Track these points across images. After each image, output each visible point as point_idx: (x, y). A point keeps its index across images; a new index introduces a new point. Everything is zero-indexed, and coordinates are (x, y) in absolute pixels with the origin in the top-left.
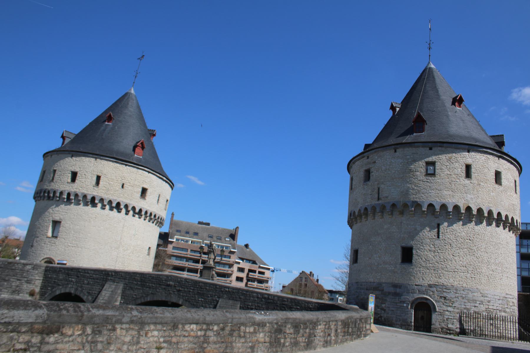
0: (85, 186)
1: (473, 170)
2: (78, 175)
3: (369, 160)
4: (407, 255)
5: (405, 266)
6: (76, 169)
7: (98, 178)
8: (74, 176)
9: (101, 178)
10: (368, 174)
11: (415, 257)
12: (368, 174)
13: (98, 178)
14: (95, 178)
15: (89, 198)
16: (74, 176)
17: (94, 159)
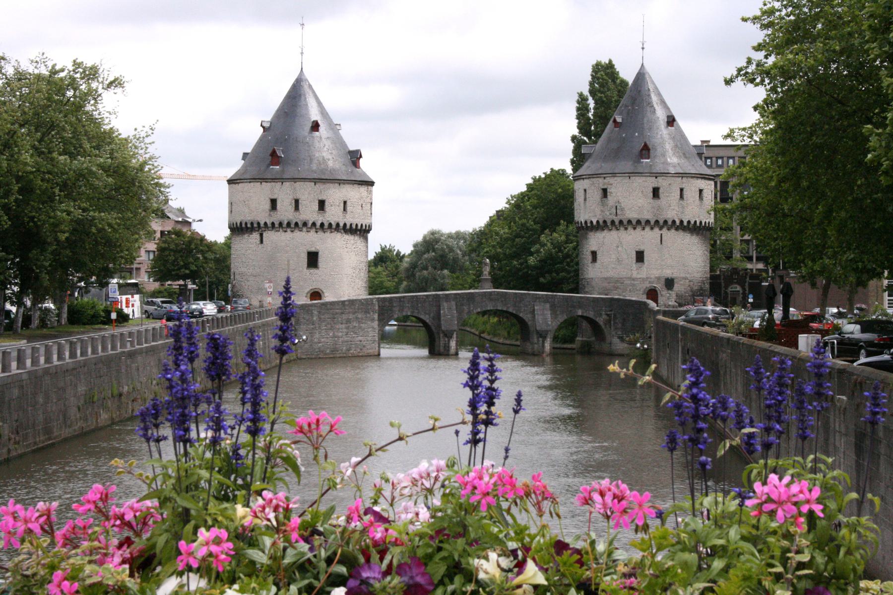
0: (333, 214)
1: (684, 192)
2: (326, 204)
3: (605, 181)
4: (640, 257)
5: (640, 264)
6: (324, 198)
7: (345, 203)
8: (322, 204)
9: (348, 203)
10: (605, 192)
11: (645, 259)
12: (605, 192)
13: (345, 203)
14: (342, 205)
15: (341, 225)
16: (322, 204)
17: (337, 185)
